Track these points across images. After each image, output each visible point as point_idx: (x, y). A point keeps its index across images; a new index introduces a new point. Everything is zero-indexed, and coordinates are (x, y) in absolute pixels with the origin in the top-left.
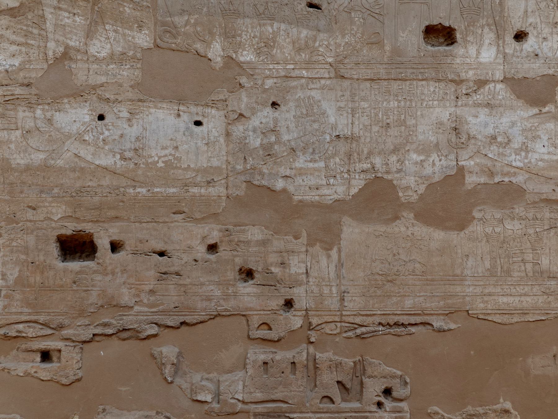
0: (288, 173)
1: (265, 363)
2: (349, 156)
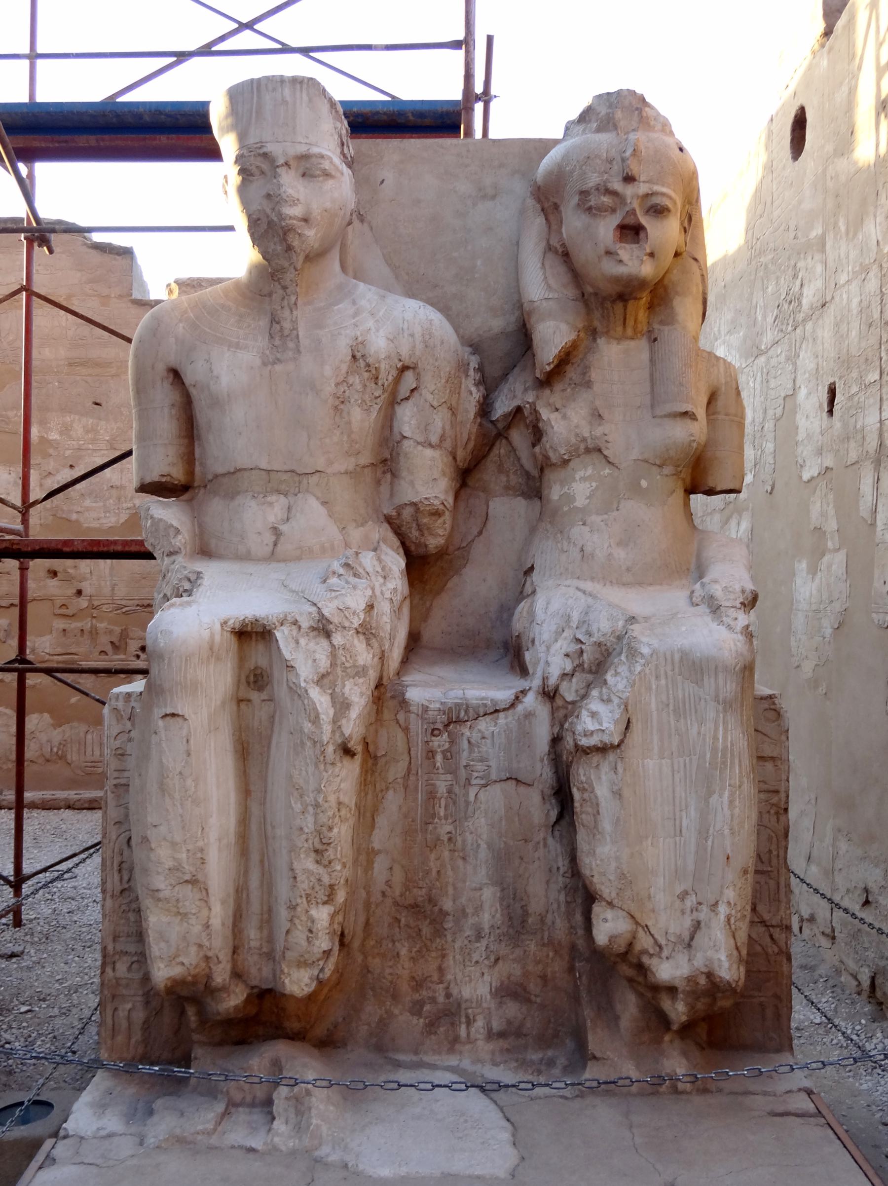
0: (79, 509)
1: (64, 630)
2: (119, 499)
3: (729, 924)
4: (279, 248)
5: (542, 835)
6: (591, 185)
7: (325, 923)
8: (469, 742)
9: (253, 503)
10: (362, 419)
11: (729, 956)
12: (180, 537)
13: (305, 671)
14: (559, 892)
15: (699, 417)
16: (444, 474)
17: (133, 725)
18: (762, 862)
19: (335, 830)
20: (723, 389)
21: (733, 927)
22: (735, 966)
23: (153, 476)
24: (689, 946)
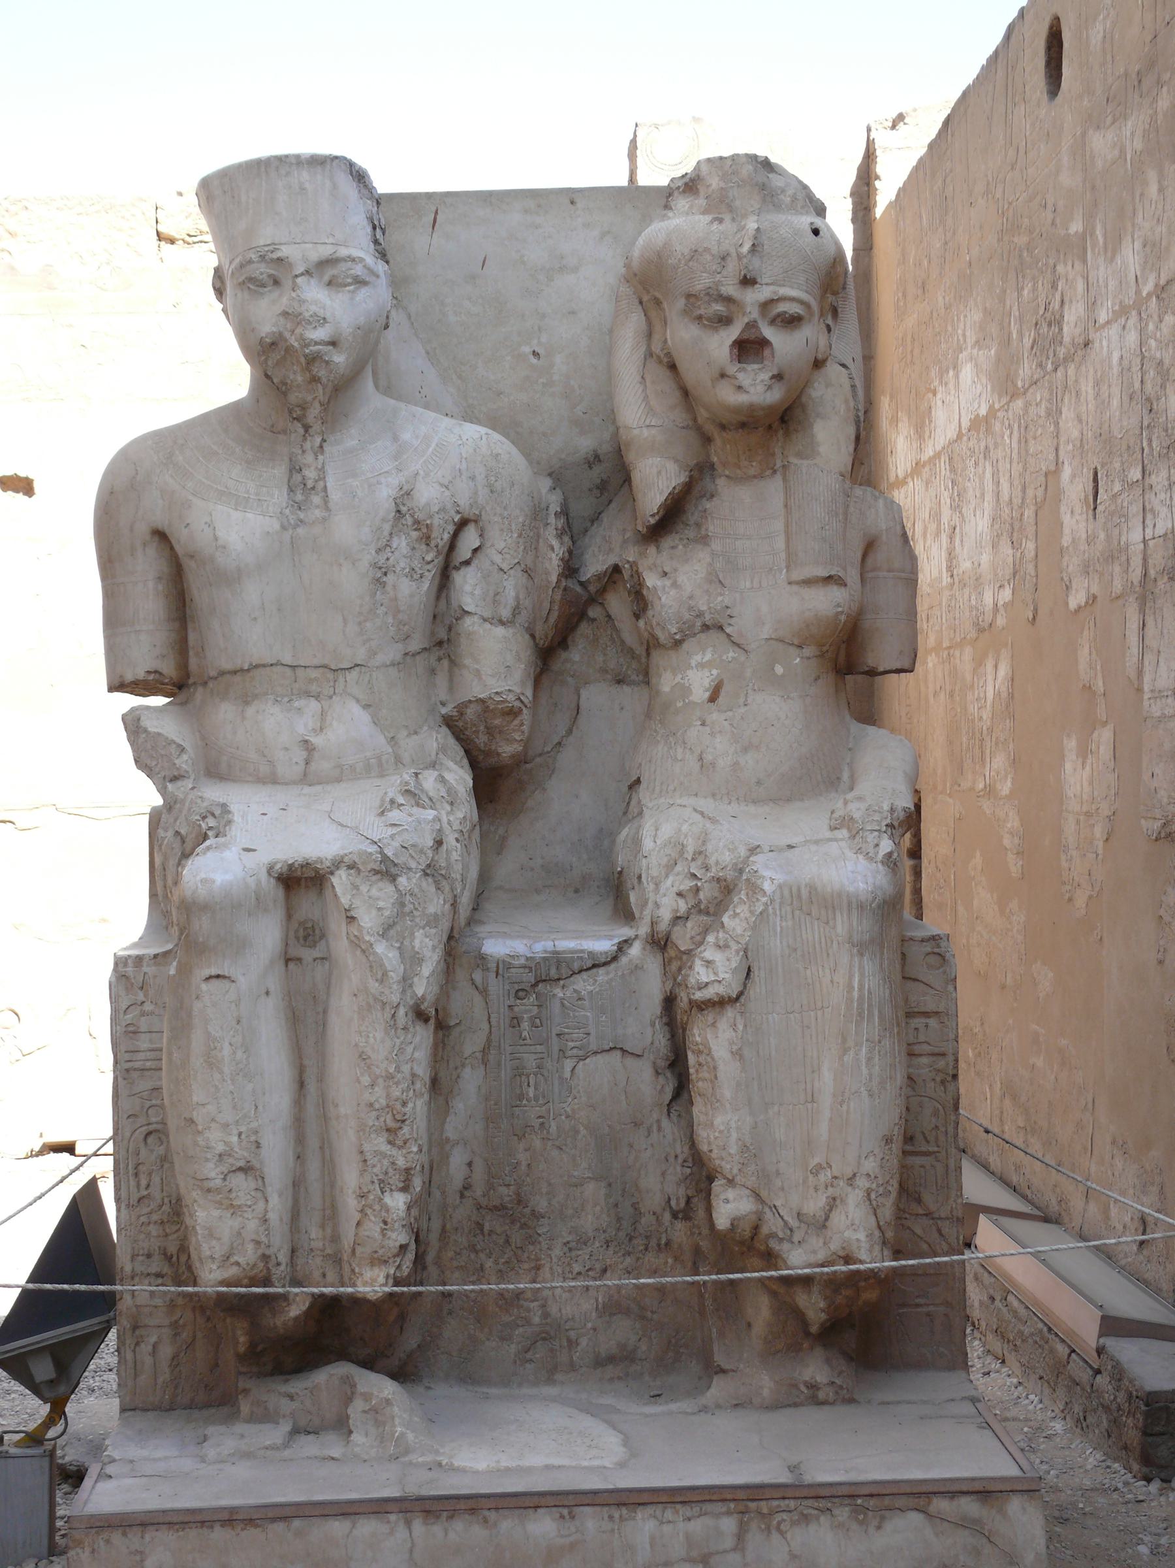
3: (870, 1200)
4: (300, 379)
5: (655, 1116)
6: (699, 287)
7: (402, 1214)
8: (563, 1005)
9: (276, 710)
10: (411, 591)
11: (870, 1236)
12: (185, 757)
13: (368, 920)
14: (678, 1184)
15: (849, 581)
16: (519, 660)
17: (145, 996)
18: (928, 1142)
19: (410, 1105)
20: (884, 537)
21: (874, 1203)
22: (877, 1248)
23: (139, 672)
24: (824, 1226)
